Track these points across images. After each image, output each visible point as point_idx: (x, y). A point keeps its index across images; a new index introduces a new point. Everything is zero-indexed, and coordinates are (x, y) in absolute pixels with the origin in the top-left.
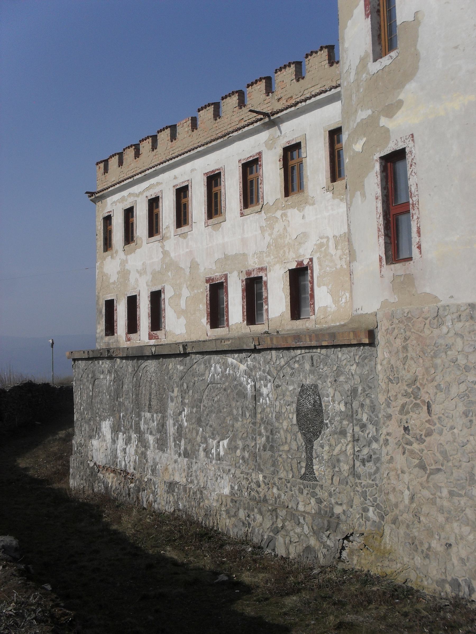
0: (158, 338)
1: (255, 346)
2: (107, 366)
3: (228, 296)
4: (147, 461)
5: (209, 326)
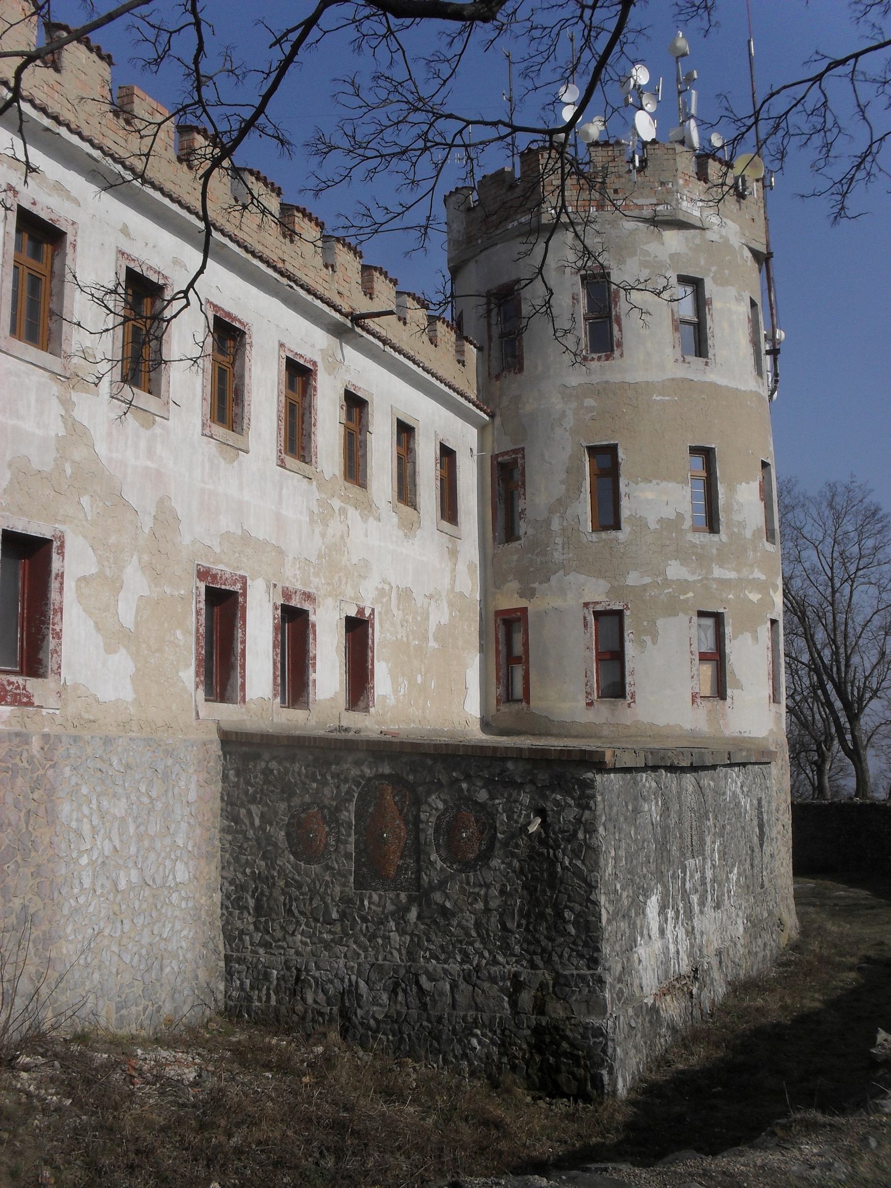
0: (30, 704)
5: (201, 694)
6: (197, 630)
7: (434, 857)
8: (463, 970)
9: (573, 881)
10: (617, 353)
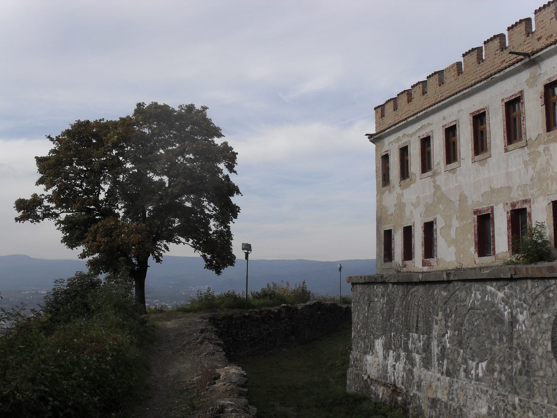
1: (511, 275)
2: (380, 290)
3: (494, 227)
4: (413, 377)
5: (476, 255)
6: (475, 232)
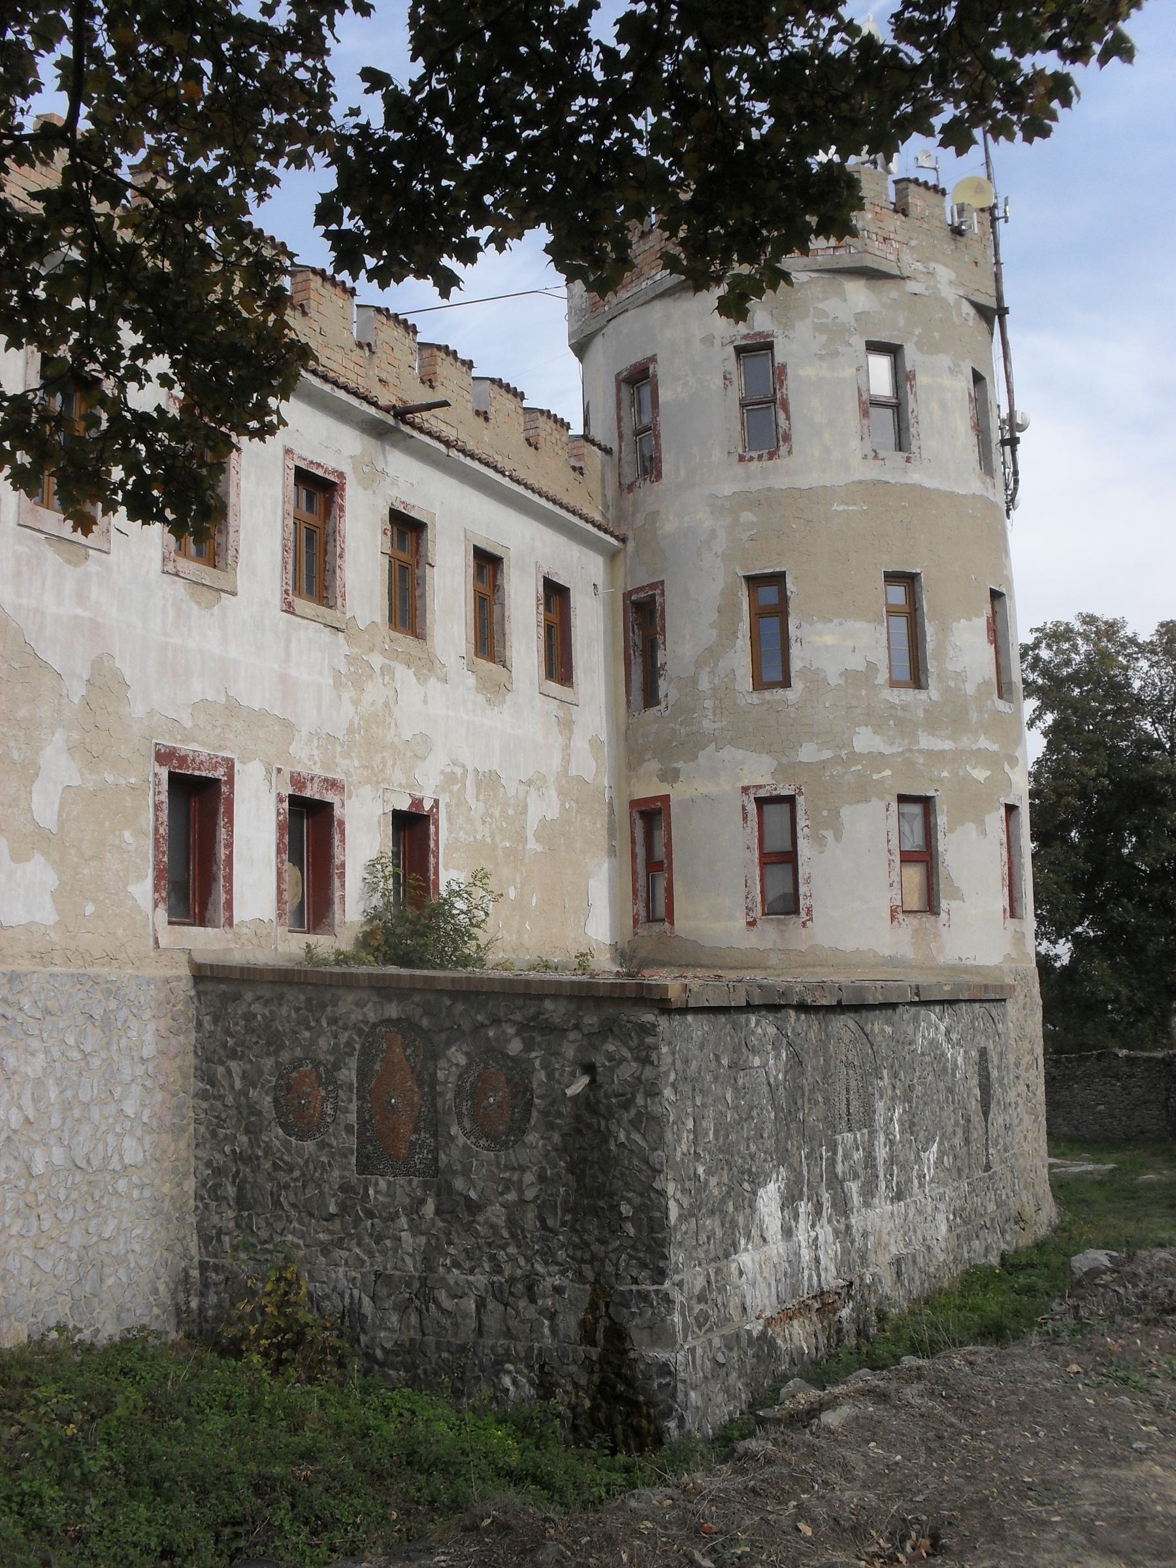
5: (162, 915)
6: (156, 830)
7: (455, 1130)
8: (492, 1284)
9: (630, 1162)
10: (783, 449)
